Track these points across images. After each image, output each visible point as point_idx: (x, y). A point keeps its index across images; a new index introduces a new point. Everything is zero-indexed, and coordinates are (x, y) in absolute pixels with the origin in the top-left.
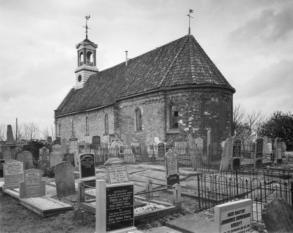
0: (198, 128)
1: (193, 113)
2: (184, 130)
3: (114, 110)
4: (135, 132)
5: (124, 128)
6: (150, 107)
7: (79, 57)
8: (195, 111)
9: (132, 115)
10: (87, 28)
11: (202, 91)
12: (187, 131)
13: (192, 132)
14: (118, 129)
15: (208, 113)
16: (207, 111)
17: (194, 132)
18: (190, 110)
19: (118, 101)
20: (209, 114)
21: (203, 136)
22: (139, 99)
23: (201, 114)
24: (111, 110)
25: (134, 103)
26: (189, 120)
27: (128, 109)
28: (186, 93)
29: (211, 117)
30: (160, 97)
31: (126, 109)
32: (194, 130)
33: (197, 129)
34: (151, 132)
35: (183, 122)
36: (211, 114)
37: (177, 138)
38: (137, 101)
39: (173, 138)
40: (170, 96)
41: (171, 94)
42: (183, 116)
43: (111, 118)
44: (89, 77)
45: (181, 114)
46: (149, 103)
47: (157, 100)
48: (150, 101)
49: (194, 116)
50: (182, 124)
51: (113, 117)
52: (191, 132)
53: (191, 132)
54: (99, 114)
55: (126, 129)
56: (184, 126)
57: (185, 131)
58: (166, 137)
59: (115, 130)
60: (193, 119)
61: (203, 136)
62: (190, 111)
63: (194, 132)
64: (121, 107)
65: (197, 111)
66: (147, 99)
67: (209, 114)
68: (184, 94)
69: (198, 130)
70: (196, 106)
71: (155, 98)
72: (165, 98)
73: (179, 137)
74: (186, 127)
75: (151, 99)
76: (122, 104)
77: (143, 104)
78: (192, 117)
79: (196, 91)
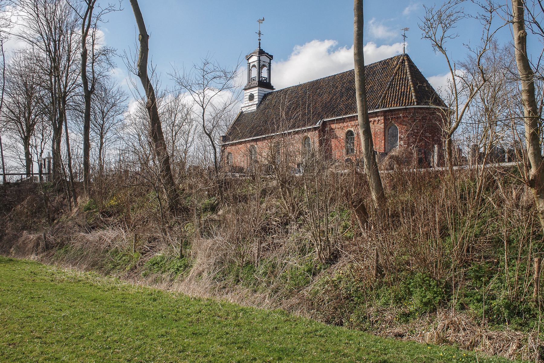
7: (250, 70)
10: (260, 34)
20: (430, 135)
44: (263, 95)
47: (375, 121)
67: (430, 135)
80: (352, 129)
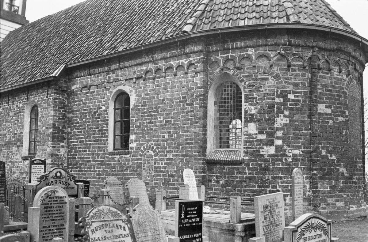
0: (299, 147)
1: (288, 106)
2: (262, 153)
3: (55, 93)
4: (110, 154)
5: (80, 142)
6: (158, 86)
8: (293, 100)
9: (104, 108)
11: (313, 47)
12: (269, 156)
13: (284, 158)
14: (62, 144)
15: (326, 107)
16: (324, 103)
17: (290, 160)
18: (278, 96)
19: (69, 73)
20: (329, 111)
21: (315, 172)
22: (125, 67)
23: (310, 110)
24: (48, 94)
25: (109, 77)
26: (276, 126)
27: (94, 92)
28: (267, 48)
29: (333, 119)
30: (191, 59)
31: (87, 93)
32: (291, 155)
33: (296, 152)
34: (156, 155)
35: (257, 128)
36: (332, 111)
37: (239, 175)
38: (120, 73)
39: (225, 173)
40: (220, 57)
41: (224, 49)
42: (259, 112)
43: (48, 115)
45: (252, 107)
46: (155, 76)
47: (180, 66)
48: (158, 70)
49: (290, 113)
50: (255, 136)
51: (52, 113)
52: (281, 160)
53: (281, 160)
54: (15, 106)
55: (84, 144)
56: (261, 140)
57: (263, 156)
58: (203, 172)
59: (53, 147)
60: (286, 121)
61: (315, 172)
62: (281, 100)
63: (290, 160)
64: (73, 88)
65: (299, 101)
66: (150, 66)
67: (329, 111)
68: (261, 51)
69: (300, 155)
70: (296, 85)
71: (174, 63)
72: (206, 62)
73: (245, 173)
74: (266, 145)
75: (162, 64)
76: (79, 80)
77: (138, 78)
78: (285, 116)
79: (297, 46)
80: (127, 89)
